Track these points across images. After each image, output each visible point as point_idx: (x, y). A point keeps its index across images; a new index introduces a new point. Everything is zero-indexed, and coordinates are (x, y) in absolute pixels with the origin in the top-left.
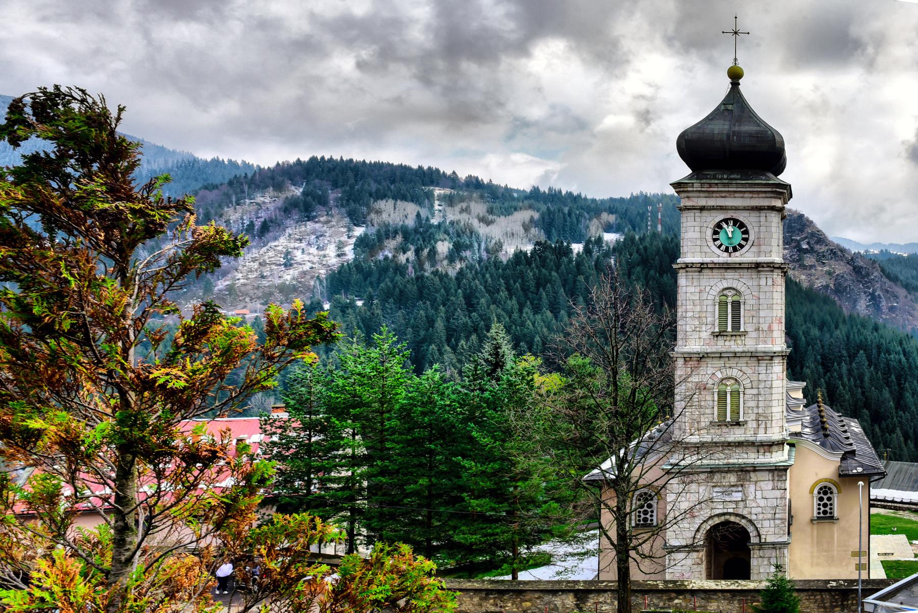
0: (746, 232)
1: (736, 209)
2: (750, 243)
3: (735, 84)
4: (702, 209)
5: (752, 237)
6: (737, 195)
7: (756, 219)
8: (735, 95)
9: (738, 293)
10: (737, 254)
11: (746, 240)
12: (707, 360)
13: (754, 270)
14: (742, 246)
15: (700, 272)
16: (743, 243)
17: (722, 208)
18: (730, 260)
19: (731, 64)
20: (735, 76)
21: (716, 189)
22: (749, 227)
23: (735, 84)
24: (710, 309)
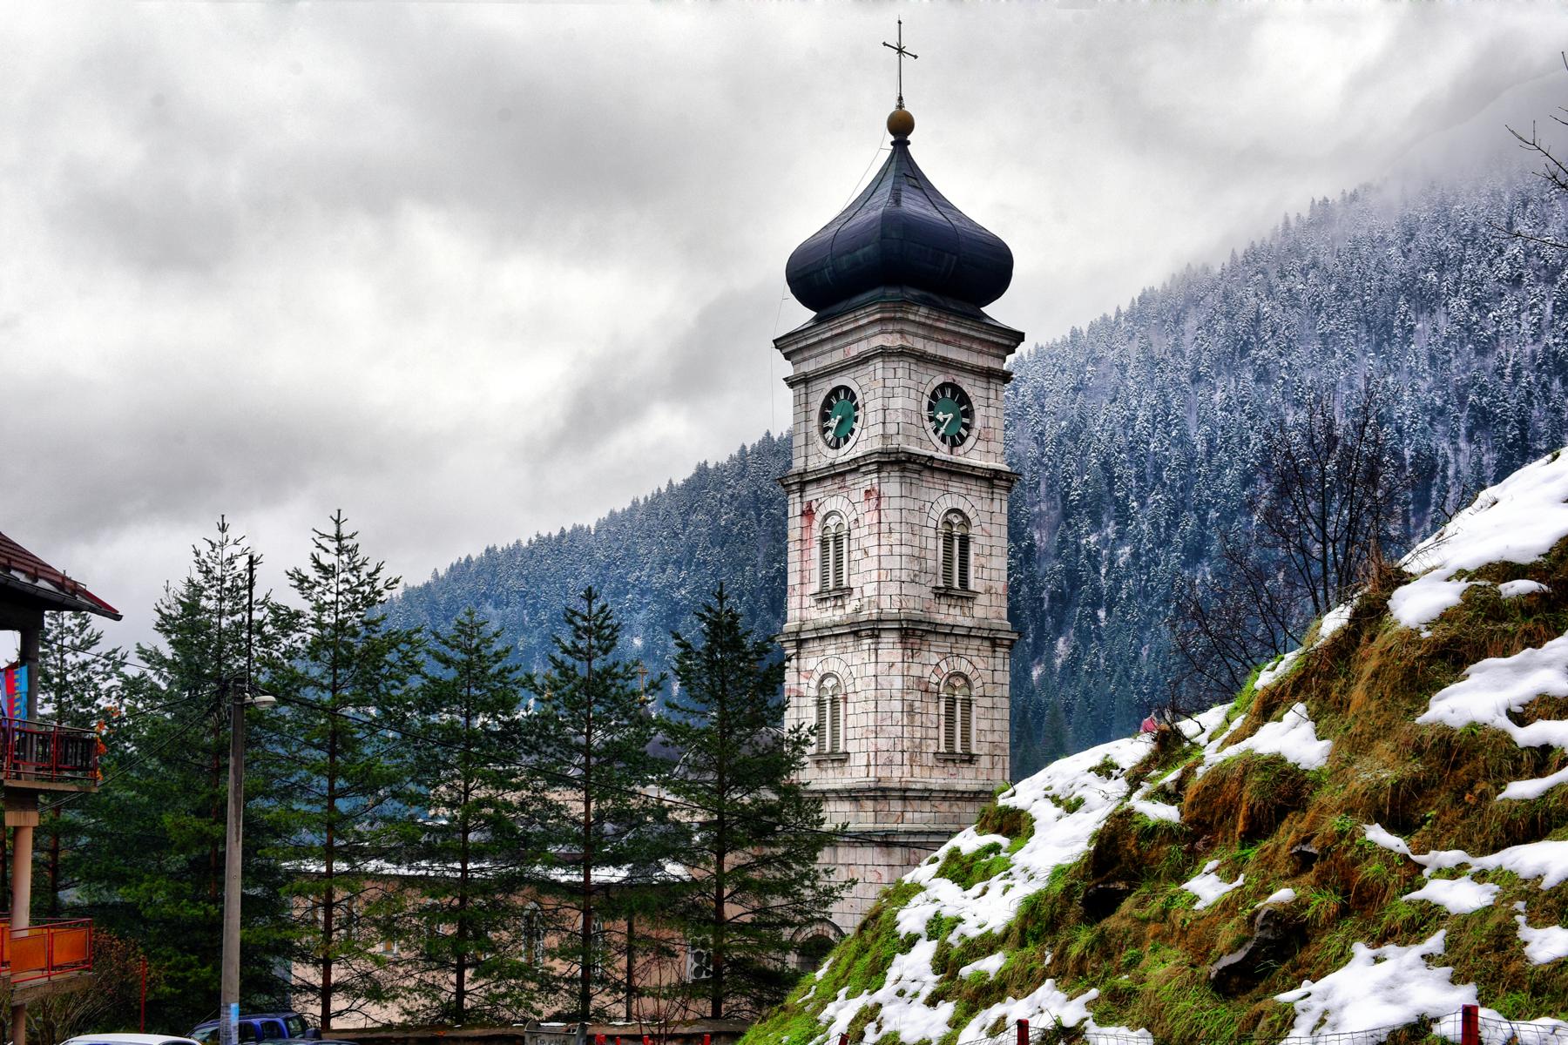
0: (969, 413)
1: (961, 367)
2: (974, 433)
3: (901, 145)
4: (922, 358)
5: (978, 423)
6: (964, 343)
7: (983, 393)
8: (902, 167)
9: (966, 522)
10: (960, 450)
11: (967, 427)
12: (931, 638)
13: (984, 484)
14: (963, 439)
15: (919, 473)
16: (963, 432)
17: (945, 363)
18: (954, 458)
19: (892, 108)
20: (901, 126)
21: (943, 325)
22: (975, 405)
23: (901, 145)
24: (931, 544)
